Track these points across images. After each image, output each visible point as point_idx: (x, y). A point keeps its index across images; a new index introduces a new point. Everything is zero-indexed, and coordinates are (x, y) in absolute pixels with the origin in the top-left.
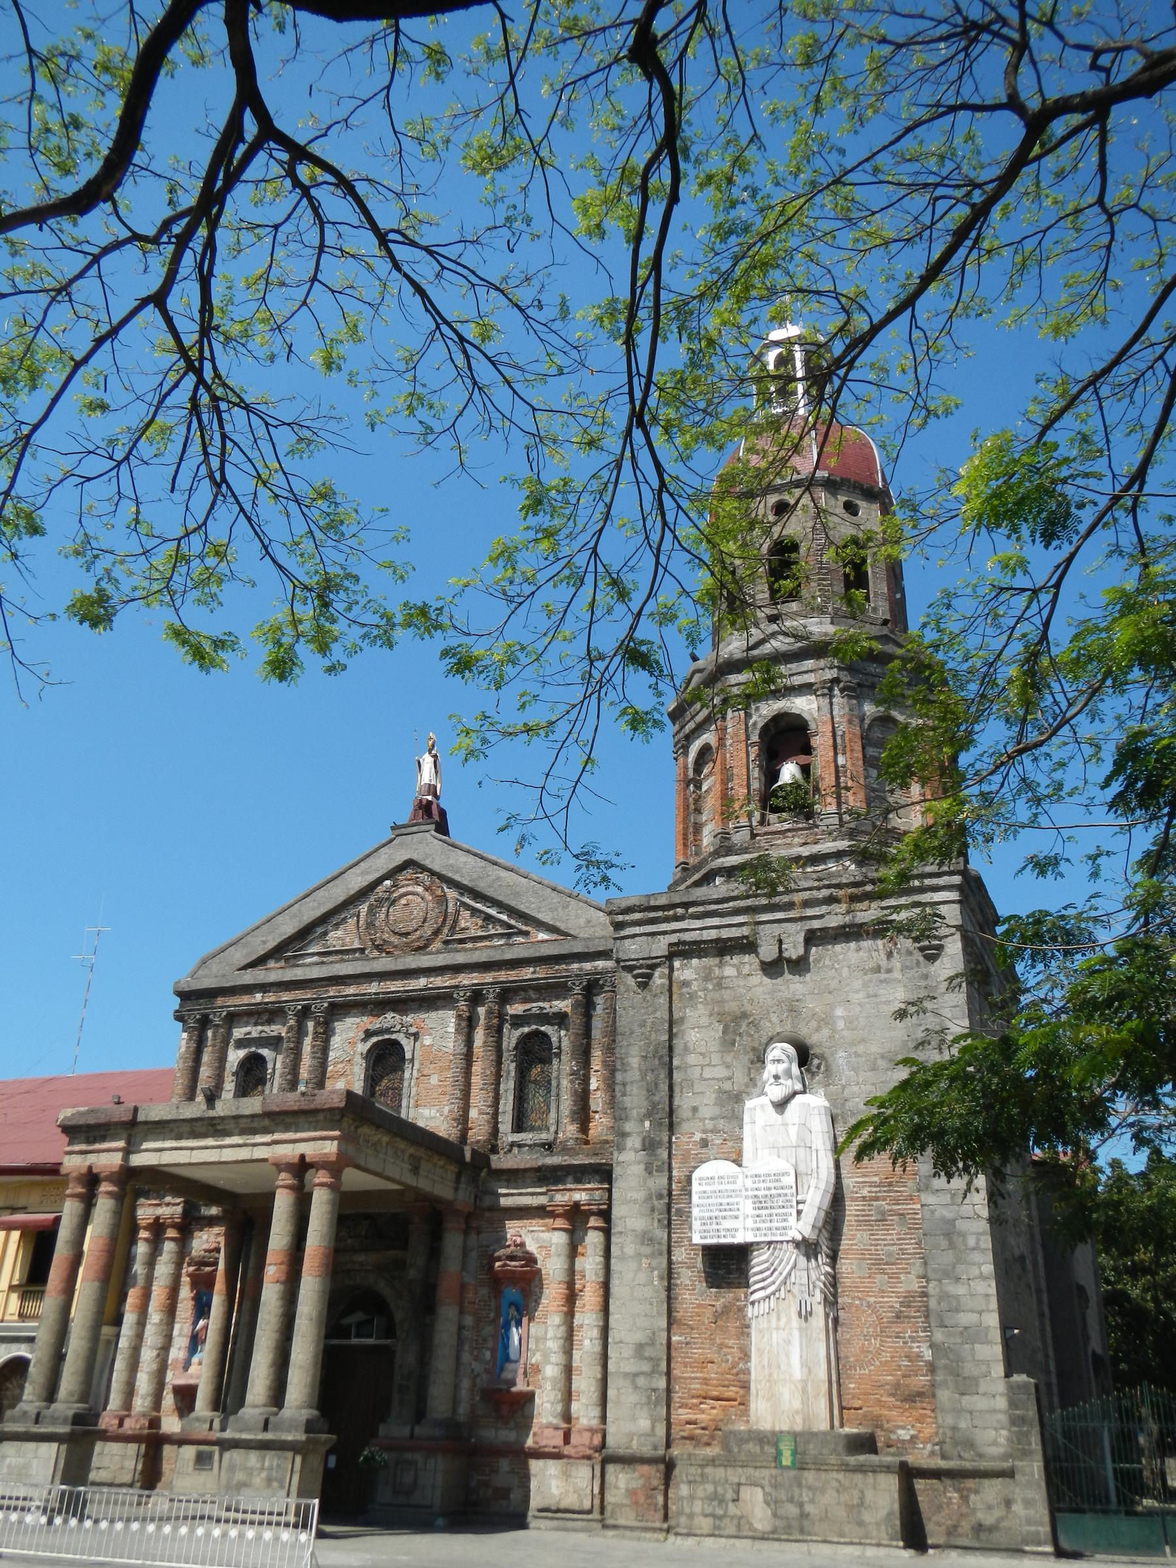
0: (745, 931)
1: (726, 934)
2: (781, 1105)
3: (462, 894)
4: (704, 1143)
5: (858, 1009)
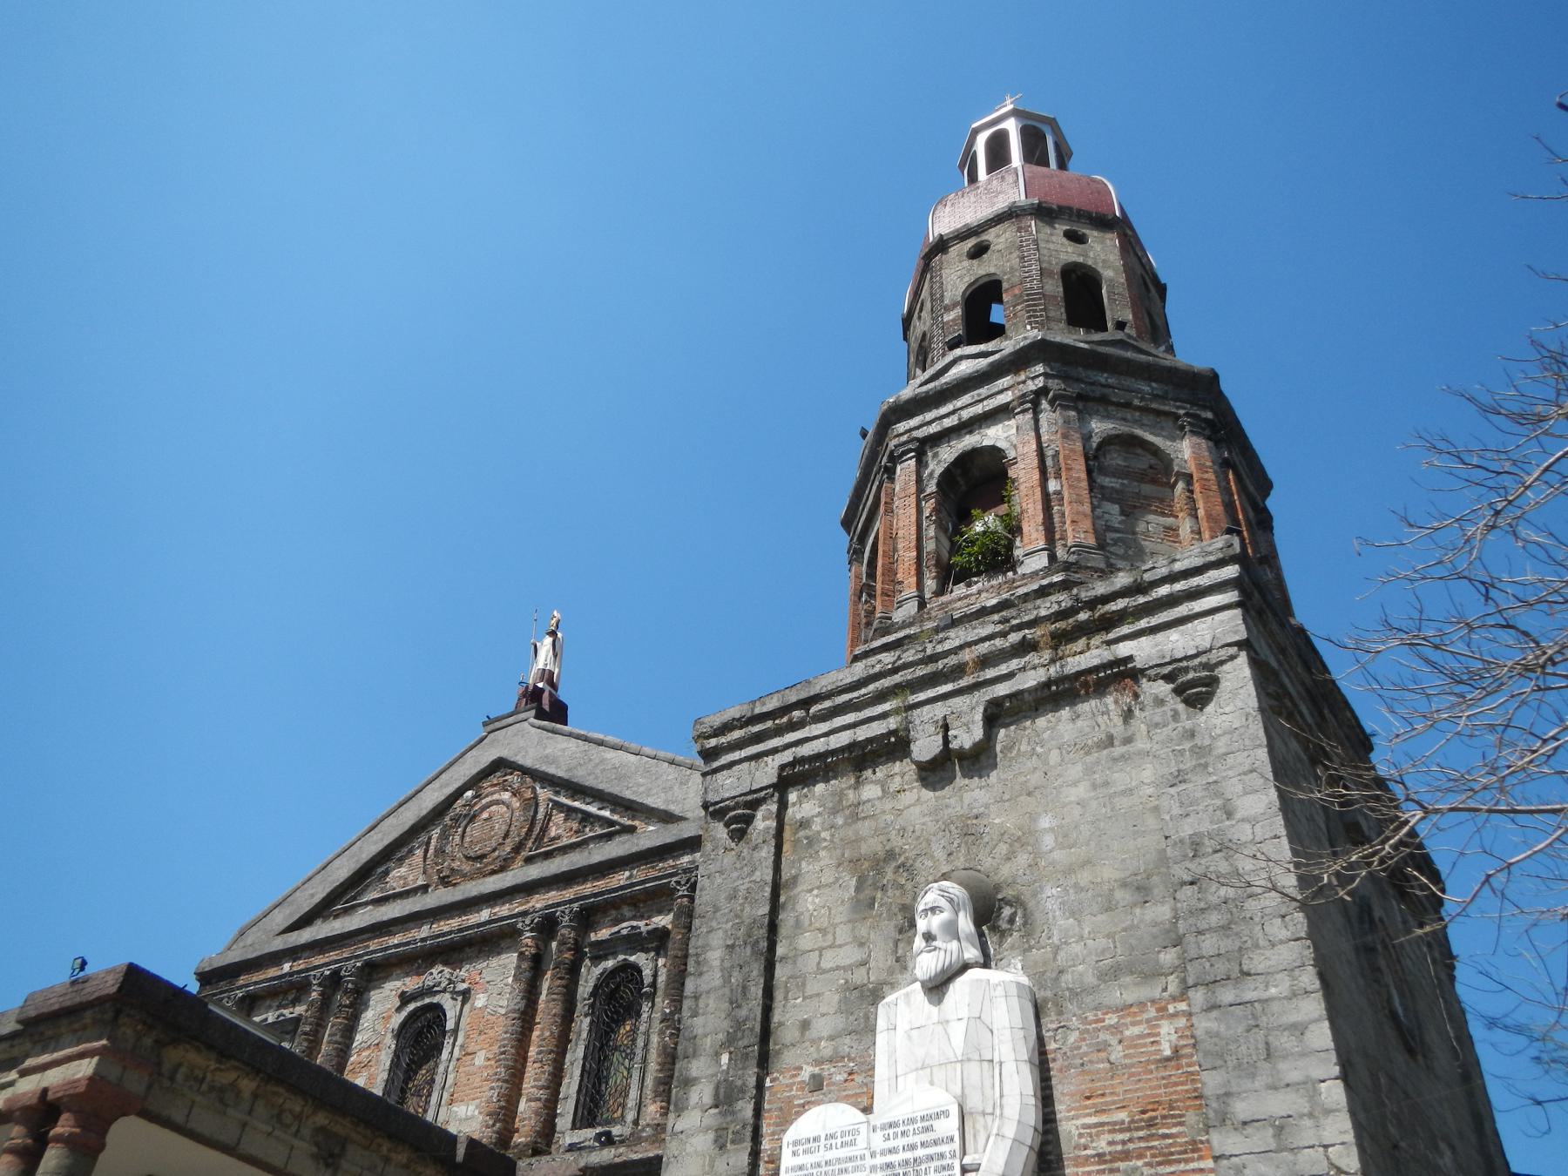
0: (892, 723)
1: (863, 733)
2: (937, 987)
3: (557, 793)
4: (817, 1084)
5: (1077, 811)
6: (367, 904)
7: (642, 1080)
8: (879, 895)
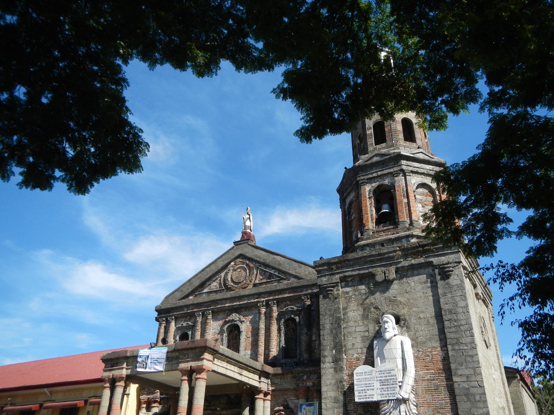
6: (205, 293)
7: (300, 347)
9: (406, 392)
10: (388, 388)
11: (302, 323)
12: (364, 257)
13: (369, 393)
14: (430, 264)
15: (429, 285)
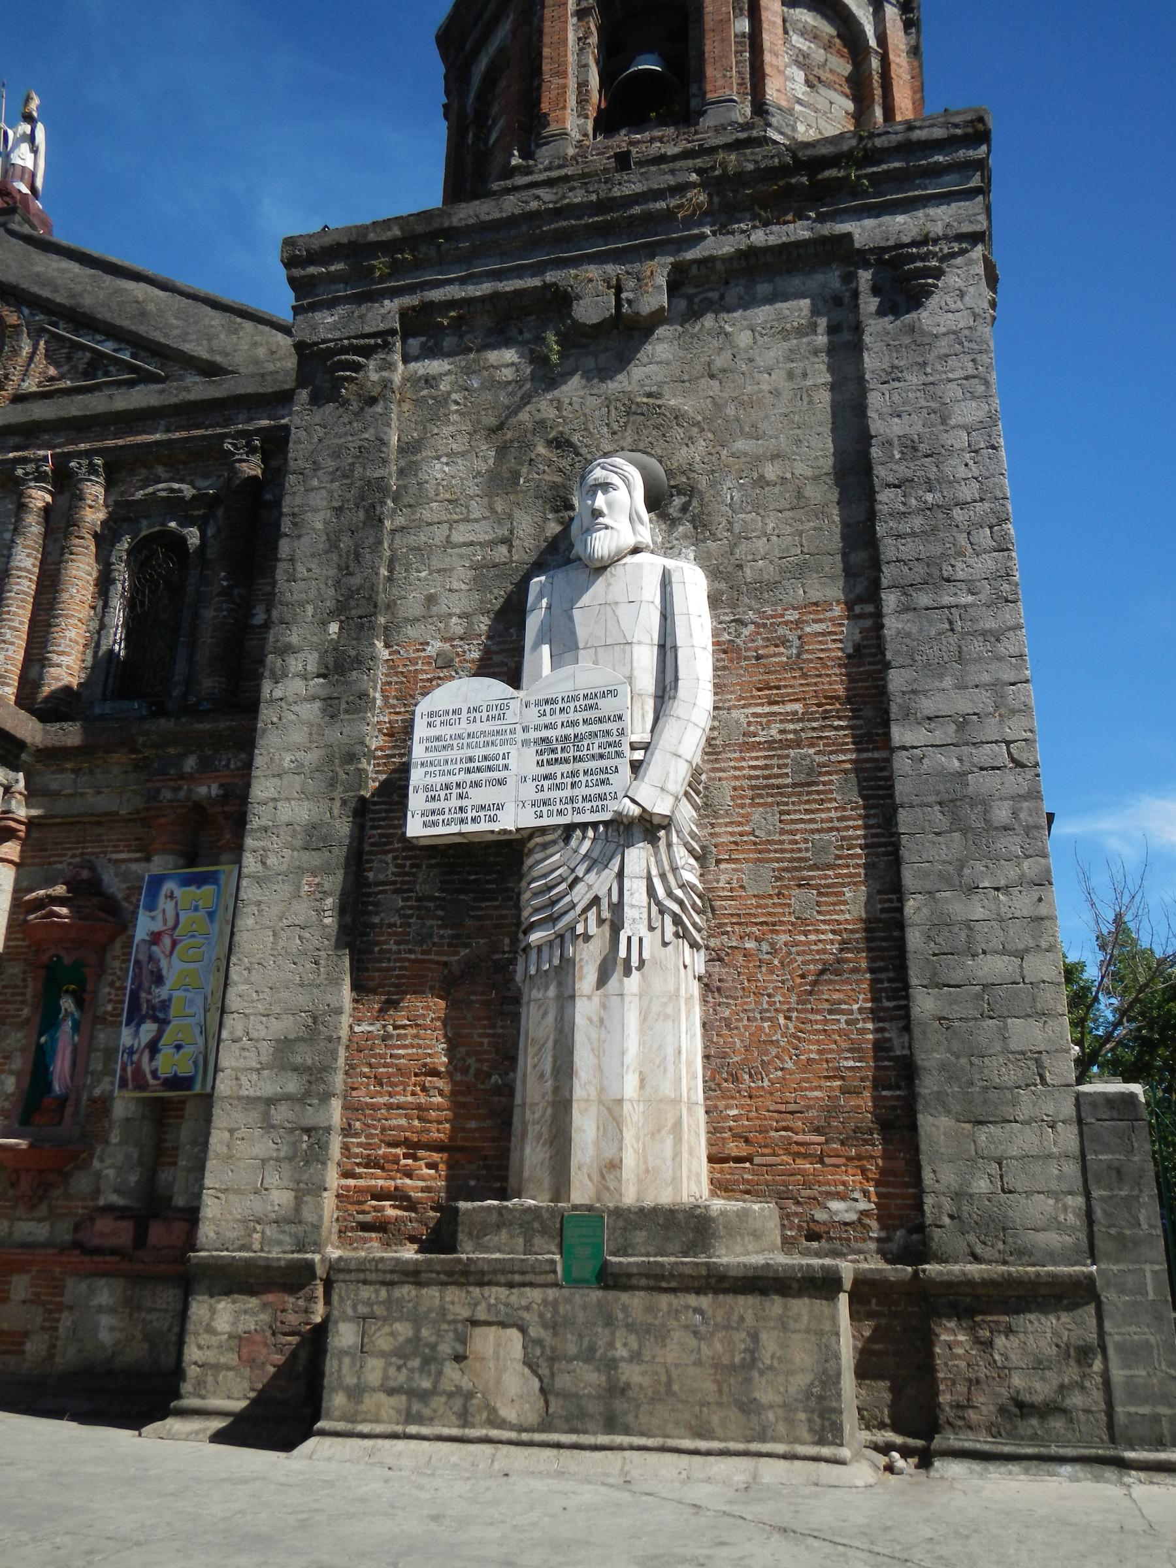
8: (524, 470)
9: (661, 790)
10: (574, 774)
11: (211, 553)
12: (531, 217)
13: (479, 796)
14: (840, 252)
15: (822, 339)
